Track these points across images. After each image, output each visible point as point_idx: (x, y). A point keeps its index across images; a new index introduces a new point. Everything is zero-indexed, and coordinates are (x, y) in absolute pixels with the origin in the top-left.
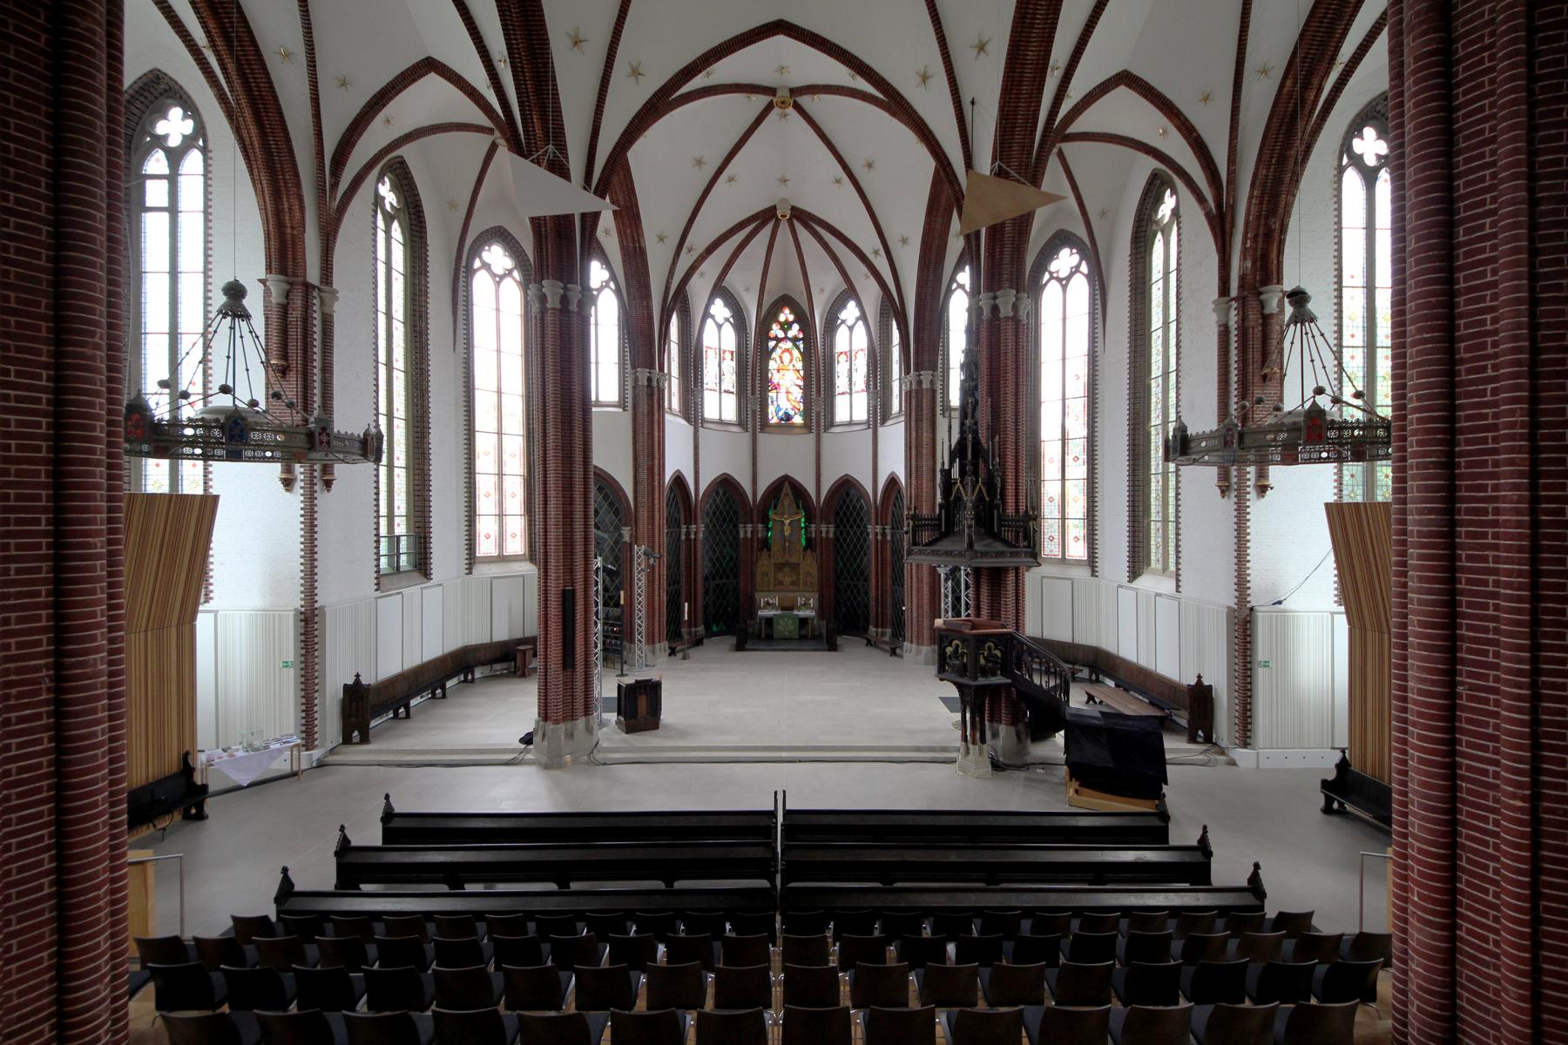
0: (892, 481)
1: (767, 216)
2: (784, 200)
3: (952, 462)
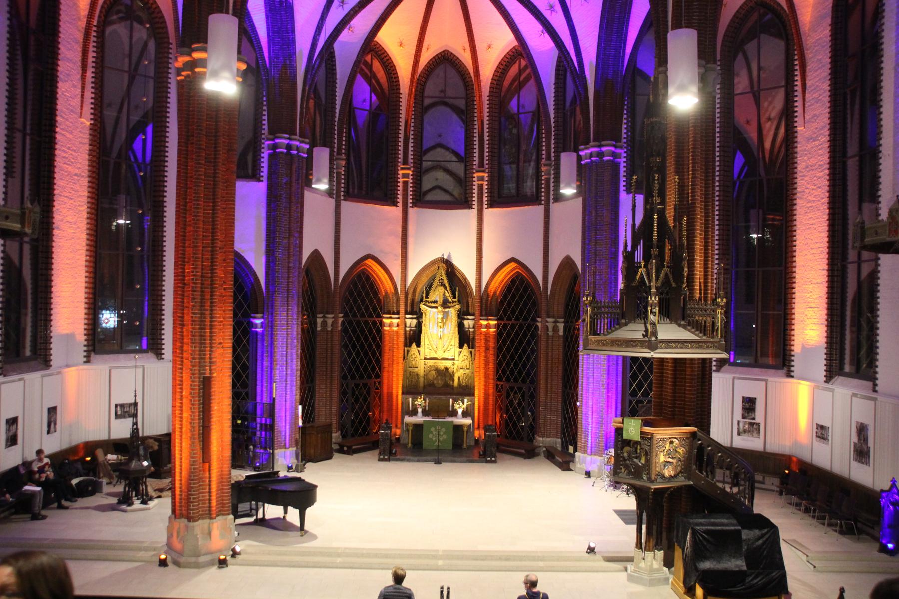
0: (568, 262)
3: (635, 246)
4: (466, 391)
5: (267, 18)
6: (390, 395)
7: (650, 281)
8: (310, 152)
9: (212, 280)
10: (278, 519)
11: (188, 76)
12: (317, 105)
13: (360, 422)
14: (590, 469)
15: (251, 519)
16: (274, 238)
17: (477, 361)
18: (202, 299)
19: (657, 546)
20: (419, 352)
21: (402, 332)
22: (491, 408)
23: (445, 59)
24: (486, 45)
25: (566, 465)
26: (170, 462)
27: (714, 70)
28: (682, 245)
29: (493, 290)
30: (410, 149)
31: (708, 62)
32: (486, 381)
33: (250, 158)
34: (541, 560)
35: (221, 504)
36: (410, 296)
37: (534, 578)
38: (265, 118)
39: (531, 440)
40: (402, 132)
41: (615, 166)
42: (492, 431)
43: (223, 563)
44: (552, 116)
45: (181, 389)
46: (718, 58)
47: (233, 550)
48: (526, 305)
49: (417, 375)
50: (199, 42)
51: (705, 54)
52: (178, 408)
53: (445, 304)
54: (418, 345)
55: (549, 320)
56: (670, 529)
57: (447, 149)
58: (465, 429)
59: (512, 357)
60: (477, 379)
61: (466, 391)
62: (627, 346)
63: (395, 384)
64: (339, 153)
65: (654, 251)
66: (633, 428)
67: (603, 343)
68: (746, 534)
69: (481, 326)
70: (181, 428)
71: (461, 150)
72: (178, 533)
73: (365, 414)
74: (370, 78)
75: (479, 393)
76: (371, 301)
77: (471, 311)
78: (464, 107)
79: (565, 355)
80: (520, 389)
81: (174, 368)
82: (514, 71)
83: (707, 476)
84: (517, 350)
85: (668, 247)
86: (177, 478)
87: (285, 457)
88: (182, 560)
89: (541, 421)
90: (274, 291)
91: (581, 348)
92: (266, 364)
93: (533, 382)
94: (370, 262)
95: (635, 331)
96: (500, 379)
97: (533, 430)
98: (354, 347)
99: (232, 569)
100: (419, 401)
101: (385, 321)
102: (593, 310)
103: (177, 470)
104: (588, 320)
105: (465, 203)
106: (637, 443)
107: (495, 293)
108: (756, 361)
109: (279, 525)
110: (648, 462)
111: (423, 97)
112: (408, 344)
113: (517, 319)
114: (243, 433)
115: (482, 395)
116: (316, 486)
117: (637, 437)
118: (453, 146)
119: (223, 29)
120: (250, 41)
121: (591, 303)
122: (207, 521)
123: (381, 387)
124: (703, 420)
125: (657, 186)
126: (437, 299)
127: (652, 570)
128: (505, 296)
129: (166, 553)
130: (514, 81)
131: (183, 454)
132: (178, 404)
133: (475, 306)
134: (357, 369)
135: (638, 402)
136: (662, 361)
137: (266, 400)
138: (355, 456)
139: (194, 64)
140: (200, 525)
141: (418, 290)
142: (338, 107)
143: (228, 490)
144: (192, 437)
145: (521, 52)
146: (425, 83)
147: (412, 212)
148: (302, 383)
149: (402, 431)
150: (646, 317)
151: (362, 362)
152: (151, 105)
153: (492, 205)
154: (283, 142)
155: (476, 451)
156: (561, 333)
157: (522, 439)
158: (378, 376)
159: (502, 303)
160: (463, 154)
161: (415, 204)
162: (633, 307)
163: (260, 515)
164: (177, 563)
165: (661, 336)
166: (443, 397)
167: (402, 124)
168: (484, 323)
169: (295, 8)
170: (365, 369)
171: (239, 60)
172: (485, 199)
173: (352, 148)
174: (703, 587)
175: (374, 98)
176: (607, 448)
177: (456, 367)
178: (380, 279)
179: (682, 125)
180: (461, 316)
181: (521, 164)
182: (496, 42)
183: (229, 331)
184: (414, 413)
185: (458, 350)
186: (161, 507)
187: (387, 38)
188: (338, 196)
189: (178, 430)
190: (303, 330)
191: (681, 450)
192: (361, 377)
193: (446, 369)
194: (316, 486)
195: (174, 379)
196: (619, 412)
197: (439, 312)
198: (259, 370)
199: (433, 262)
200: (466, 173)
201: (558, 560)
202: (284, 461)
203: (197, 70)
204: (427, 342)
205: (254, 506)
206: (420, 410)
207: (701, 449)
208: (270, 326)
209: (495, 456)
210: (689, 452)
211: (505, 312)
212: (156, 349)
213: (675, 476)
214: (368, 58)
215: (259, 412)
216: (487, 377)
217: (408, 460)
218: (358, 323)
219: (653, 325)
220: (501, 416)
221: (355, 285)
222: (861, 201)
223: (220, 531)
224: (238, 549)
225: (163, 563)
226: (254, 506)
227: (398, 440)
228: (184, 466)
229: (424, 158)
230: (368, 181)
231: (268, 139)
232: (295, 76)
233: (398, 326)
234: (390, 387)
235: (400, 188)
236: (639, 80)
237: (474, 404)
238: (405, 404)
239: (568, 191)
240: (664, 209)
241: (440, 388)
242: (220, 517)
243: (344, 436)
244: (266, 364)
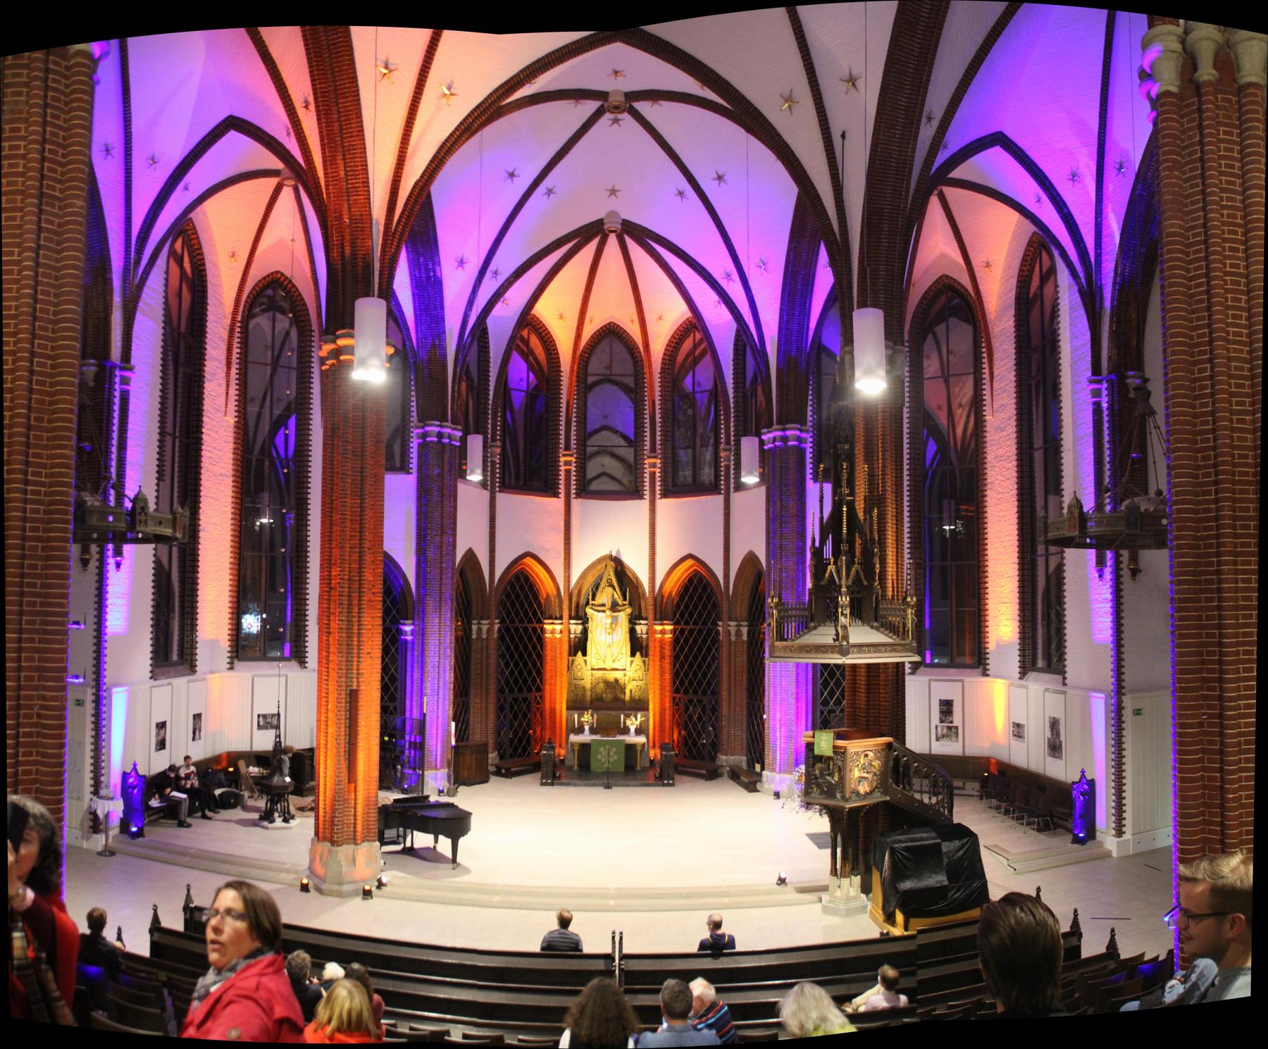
0: (751, 558)
1: (593, 232)
2: (613, 214)
3: (823, 542)
4: (639, 705)
5: (413, 295)
6: (553, 711)
7: (840, 579)
8: (464, 440)
10: (428, 848)
11: (333, 365)
12: (469, 387)
13: (520, 741)
14: (779, 789)
15: (399, 848)
16: (425, 536)
18: (350, 605)
19: (854, 871)
21: (566, 639)
22: (667, 723)
23: (611, 332)
24: (656, 316)
25: (752, 786)
26: (312, 779)
27: (901, 352)
28: (872, 540)
30: (573, 433)
31: (895, 344)
33: (397, 448)
34: (727, 896)
35: (367, 829)
36: (574, 599)
37: (717, 918)
38: (414, 404)
39: (713, 759)
40: (563, 414)
41: (800, 452)
42: (669, 750)
43: (367, 894)
44: (731, 395)
46: (906, 337)
47: (379, 881)
48: (705, 607)
50: (343, 328)
51: (892, 334)
53: (614, 607)
54: (584, 654)
56: (866, 852)
57: (615, 431)
58: (639, 748)
59: (691, 666)
60: (651, 692)
61: (639, 705)
62: (817, 652)
63: (558, 697)
64: (494, 440)
65: (844, 547)
66: (825, 743)
67: (791, 649)
68: (946, 847)
69: (655, 632)
71: (630, 433)
72: (321, 856)
73: (525, 732)
74: (527, 354)
75: (653, 707)
76: (531, 605)
77: (644, 615)
78: (632, 385)
79: (750, 661)
80: (700, 702)
81: (319, 678)
82: (688, 344)
83: (904, 788)
84: (695, 658)
85: (858, 542)
86: (321, 798)
87: (436, 779)
88: (325, 887)
89: (724, 737)
90: (425, 595)
91: (767, 655)
92: (417, 675)
93: (714, 693)
94: (529, 561)
95: (824, 635)
96: (677, 691)
97: (715, 747)
98: (512, 656)
99: (376, 902)
100: (587, 717)
101: (546, 627)
102: (779, 612)
103: (321, 789)
104: (774, 624)
105: (636, 493)
106: (829, 758)
107: (670, 593)
108: (952, 661)
109: (427, 856)
110: (842, 778)
111: (586, 375)
112: (573, 652)
113: (696, 623)
114: (391, 751)
115: (657, 710)
116: (469, 814)
117: (830, 753)
118: (620, 429)
119: (370, 312)
120: (396, 321)
121: (777, 605)
122: (352, 846)
123: (543, 702)
124: (899, 731)
125: (845, 476)
126: (605, 601)
127: (848, 899)
128: (682, 597)
129: (308, 877)
130: (688, 355)
131: (327, 771)
133: (648, 610)
134: (516, 682)
135: (830, 712)
136: (854, 667)
137: (416, 715)
138: (515, 779)
139: (338, 352)
140: (345, 850)
141: (583, 592)
142: (492, 388)
143: (374, 814)
145: (695, 324)
146: (588, 359)
147: (576, 504)
148: (455, 696)
149: (568, 752)
150: (837, 619)
151: (521, 673)
152: (294, 395)
153: (665, 495)
154: (433, 429)
155: (651, 773)
156: (745, 638)
157: (703, 758)
158: (539, 689)
159: (678, 605)
160: (632, 437)
161: (578, 495)
162: (822, 608)
163: (408, 844)
164: (319, 890)
165: (853, 640)
166: (613, 713)
167: (564, 406)
168: (659, 628)
169: (444, 282)
170: (525, 681)
171: (388, 344)
172: (658, 488)
173: (508, 431)
174: (904, 913)
175: (532, 376)
176: (797, 765)
179: (869, 411)
180: (633, 620)
181: (698, 449)
182: (666, 313)
183: (378, 640)
184: (580, 730)
185: (630, 659)
186: (303, 826)
187: (545, 310)
188: (493, 488)
189: (322, 746)
190: (456, 637)
191: (876, 763)
192: (520, 691)
193: (616, 681)
194: (469, 814)
195: (319, 691)
196: (810, 725)
198: (408, 683)
199: (600, 561)
200: (636, 460)
201: (746, 894)
202: (435, 784)
203: (342, 358)
204: (594, 651)
205: (401, 833)
206: (587, 728)
207: (897, 760)
208: (421, 633)
209: (673, 779)
210: (885, 765)
211: (682, 615)
212: (299, 656)
213: (871, 792)
214: (525, 333)
215: (408, 728)
216: (662, 689)
217: (575, 785)
218: (517, 630)
219: (845, 627)
220: (679, 733)
221: (512, 586)
222: (1047, 493)
223: (365, 858)
224: (384, 880)
225: (305, 888)
226: (401, 833)
227: (562, 761)
229: (589, 443)
230: (527, 471)
231: (417, 427)
232: (445, 357)
234: (553, 702)
235: (562, 477)
236: (824, 356)
237: (648, 720)
238: (570, 721)
239: (750, 479)
240: (853, 502)
241: (610, 702)
242: (365, 844)
243: (501, 757)
244: (417, 675)
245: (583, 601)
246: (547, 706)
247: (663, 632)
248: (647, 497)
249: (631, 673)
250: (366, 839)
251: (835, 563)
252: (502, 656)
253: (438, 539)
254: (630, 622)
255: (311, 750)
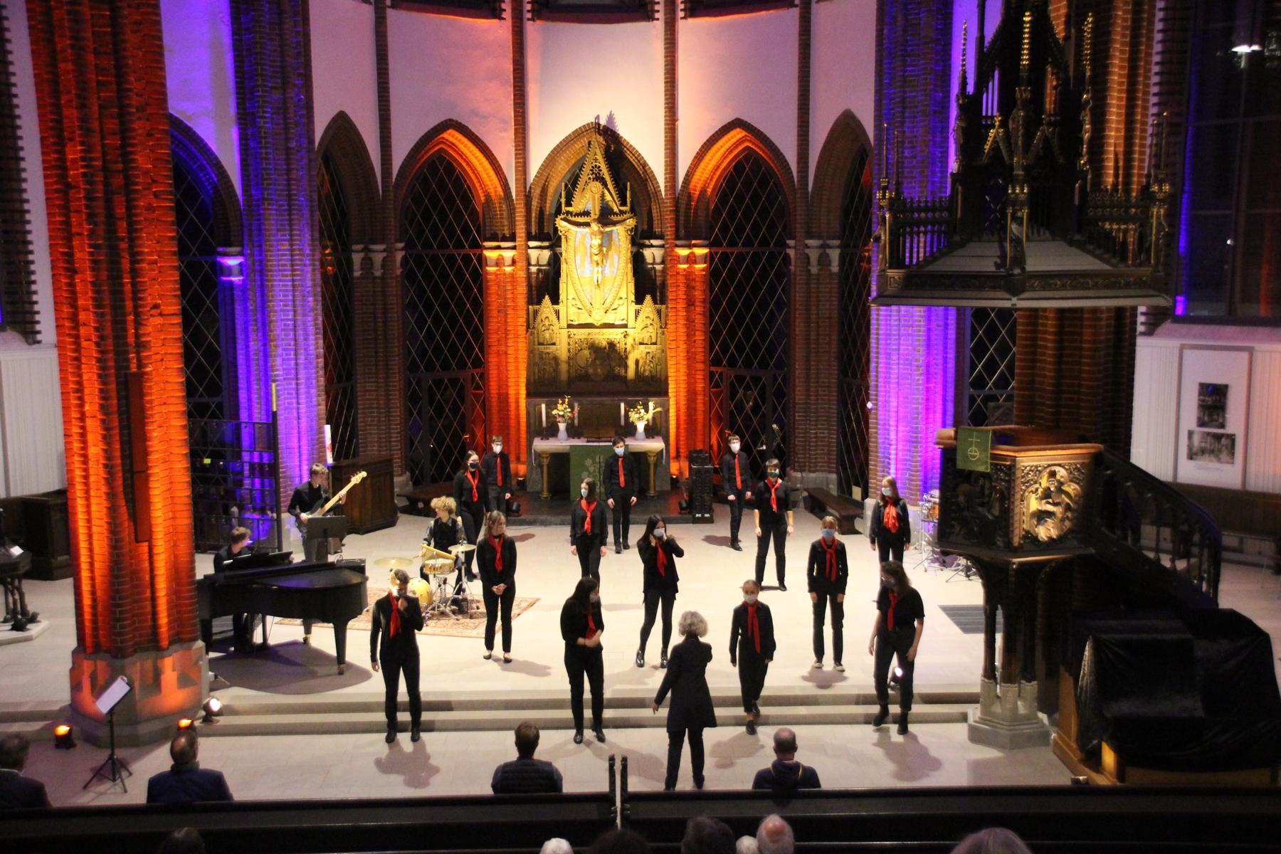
0: (847, 124)
3: (982, 83)
4: (652, 386)
6: (504, 399)
9: (127, 178)
10: (294, 644)
17: (671, 327)
20: (557, 313)
21: (522, 274)
22: (700, 417)
29: (699, 186)
32: (689, 366)
36: (535, 203)
45: (81, 398)
47: (207, 708)
49: (556, 359)
52: (76, 437)
53: (606, 217)
54: (555, 300)
55: (810, 242)
58: (652, 460)
59: (740, 318)
60: (671, 362)
61: (652, 386)
63: (513, 377)
65: (1022, 93)
69: (678, 259)
70: (86, 477)
75: (676, 388)
76: (458, 215)
77: (657, 230)
80: (756, 380)
85: (1051, 82)
86: (85, 574)
89: (798, 441)
92: (255, 345)
93: (780, 365)
94: (452, 136)
95: (981, 258)
96: (716, 361)
98: (429, 307)
100: (561, 409)
101: (487, 253)
102: (894, 217)
103: (84, 559)
107: (703, 191)
108: (1231, 311)
114: (217, 483)
115: (683, 393)
122: (153, 654)
126: (589, 207)
127: (1016, 719)
132: (75, 430)
133: (665, 220)
135: (988, 399)
137: (259, 416)
144: (111, 496)
147: (533, 30)
148: (329, 381)
150: (1004, 229)
151: (446, 336)
155: (674, 503)
156: (835, 268)
158: (479, 363)
161: (538, 14)
165: (1033, 265)
166: (607, 400)
168: (683, 252)
174: (1118, 750)
176: (926, 489)
177: (630, 341)
178: (474, 170)
180: (639, 239)
184: (552, 431)
185: (634, 307)
189: (78, 479)
190: (324, 275)
193: (612, 345)
196: (950, 421)
197: (593, 233)
199: (578, 134)
204: (572, 294)
206: (562, 426)
208: (258, 270)
209: (710, 510)
213: (1061, 538)
215: (246, 442)
216: (690, 358)
218: (435, 260)
219: (1017, 242)
224: (215, 705)
228: (97, 550)
233: (514, 262)
234: (503, 384)
237: (667, 411)
238: (533, 415)
241: (601, 381)
243: (416, 482)
244: (255, 345)
245: (549, 208)
246: (494, 390)
247: (691, 259)
248: (660, 16)
249: (636, 330)
250: (180, 638)
251: (1004, 124)
252: (412, 307)
253: (277, 95)
254: (634, 242)
255: (61, 493)
